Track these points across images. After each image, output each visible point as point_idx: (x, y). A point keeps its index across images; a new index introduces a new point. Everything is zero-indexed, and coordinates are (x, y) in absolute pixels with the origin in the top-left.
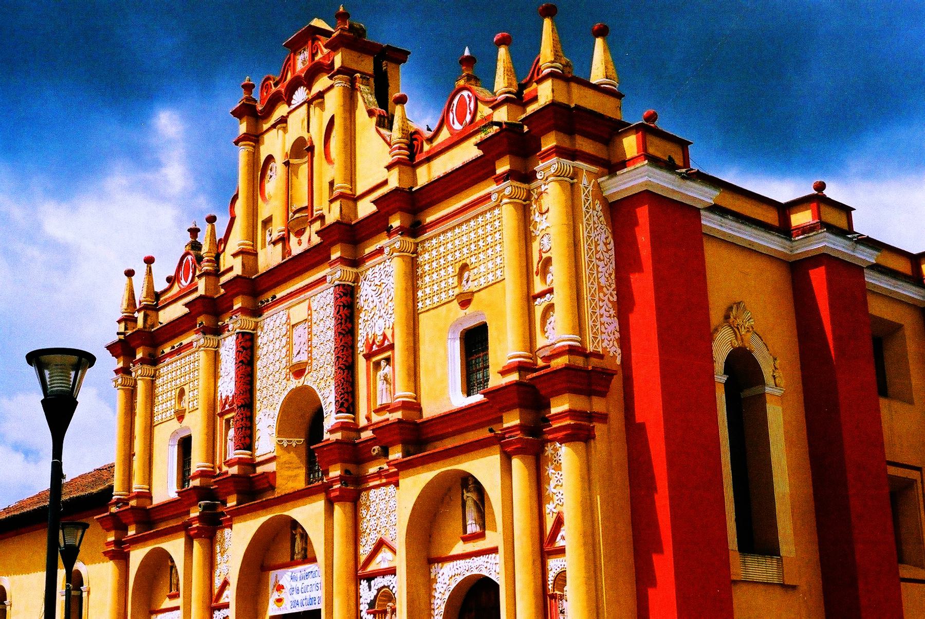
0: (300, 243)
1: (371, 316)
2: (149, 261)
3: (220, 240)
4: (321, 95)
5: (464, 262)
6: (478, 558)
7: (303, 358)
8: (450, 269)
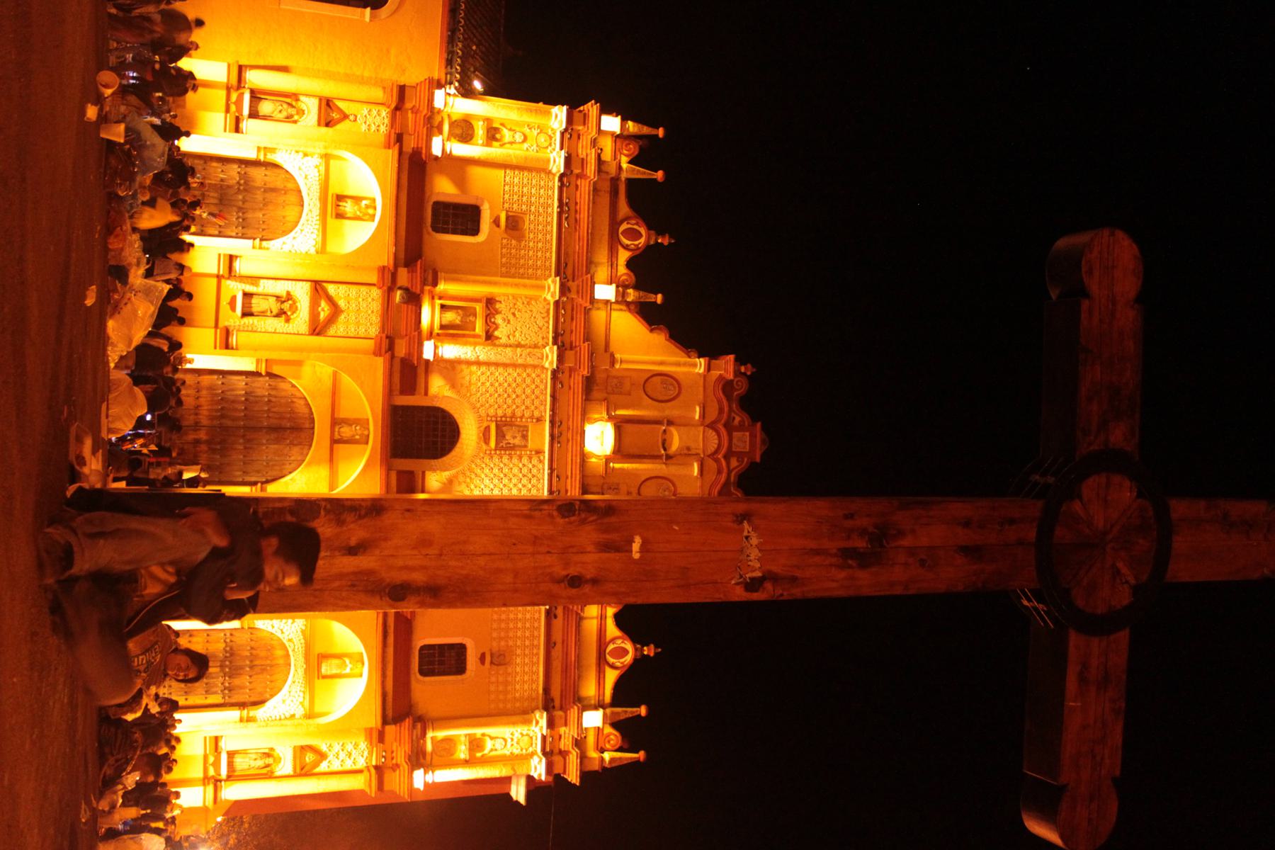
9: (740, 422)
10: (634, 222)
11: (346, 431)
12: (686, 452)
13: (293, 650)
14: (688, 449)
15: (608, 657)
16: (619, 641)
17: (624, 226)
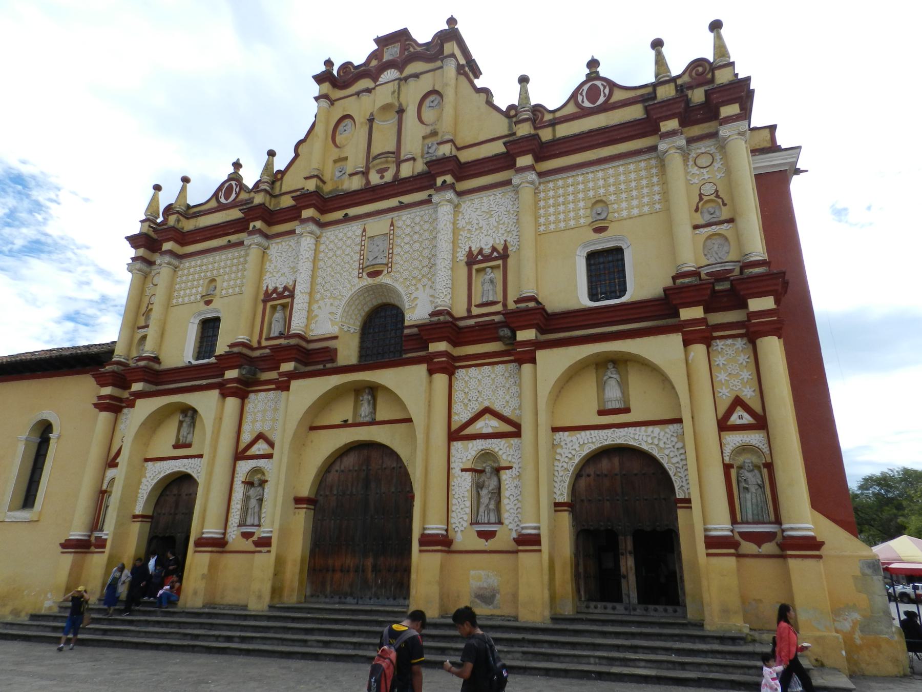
0: (382, 177)
1: (475, 234)
2: (186, 180)
3: (279, 171)
4: (416, 76)
5: (599, 199)
6: (621, 430)
7: (385, 261)
8: (581, 204)
12: (396, 93)
14: (394, 92)
15: (596, 105)
16: (580, 98)
17: (223, 200)
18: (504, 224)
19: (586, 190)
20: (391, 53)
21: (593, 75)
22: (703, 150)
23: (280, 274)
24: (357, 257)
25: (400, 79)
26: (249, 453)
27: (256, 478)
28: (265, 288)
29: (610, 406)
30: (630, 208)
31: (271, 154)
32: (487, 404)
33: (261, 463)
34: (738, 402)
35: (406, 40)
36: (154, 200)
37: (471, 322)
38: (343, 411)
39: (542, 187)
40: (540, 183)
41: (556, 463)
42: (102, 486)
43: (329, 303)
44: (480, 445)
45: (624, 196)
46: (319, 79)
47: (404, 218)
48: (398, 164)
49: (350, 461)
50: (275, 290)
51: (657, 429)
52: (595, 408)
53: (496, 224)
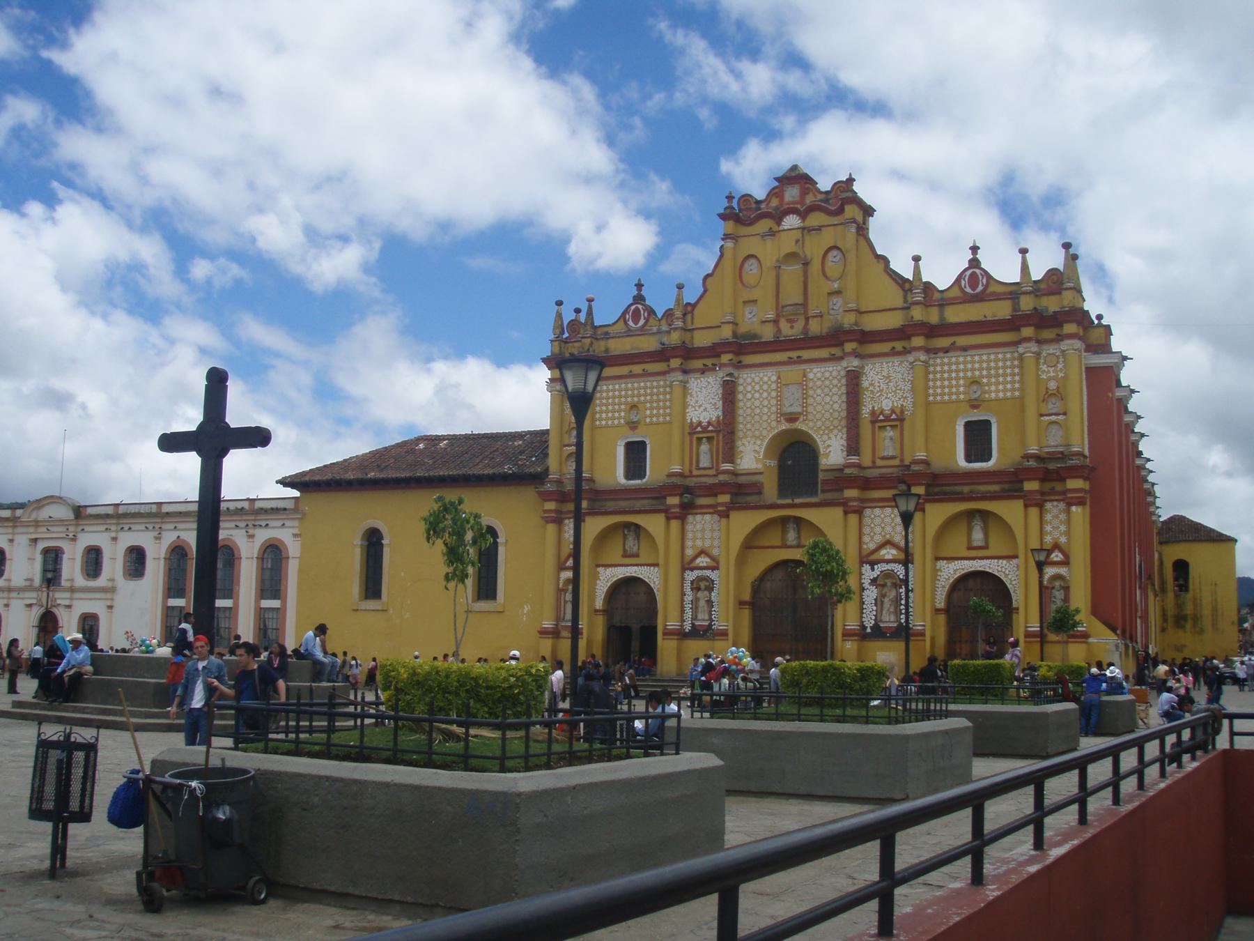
0: (792, 327)
2: (590, 300)
4: (819, 229)
7: (799, 409)
8: (962, 382)
9: (777, 197)
10: (627, 316)
11: (791, 536)
12: (801, 242)
13: (963, 569)
14: (797, 241)
16: (963, 283)
17: (631, 323)
18: (900, 389)
19: (965, 371)
20: (792, 193)
21: (975, 263)
22: (1051, 351)
23: (702, 409)
24: (774, 402)
25: (803, 228)
26: (693, 565)
27: (702, 585)
28: (689, 421)
29: (975, 544)
30: (997, 391)
31: (680, 287)
32: (888, 536)
33: (708, 573)
34: (1056, 546)
35: (806, 183)
36: (559, 316)
37: (876, 472)
38: (774, 538)
39: (931, 362)
40: (930, 358)
41: (937, 582)
42: (559, 585)
43: (752, 442)
44: (885, 567)
45: (993, 380)
46: (723, 217)
47: (815, 370)
48: (807, 319)
49: (779, 575)
50: (700, 424)
51: (1005, 562)
52: (965, 545)
53: (894, 389)
